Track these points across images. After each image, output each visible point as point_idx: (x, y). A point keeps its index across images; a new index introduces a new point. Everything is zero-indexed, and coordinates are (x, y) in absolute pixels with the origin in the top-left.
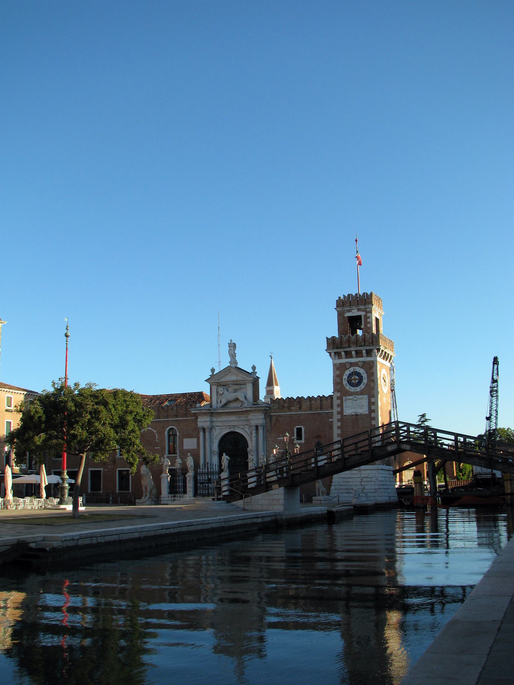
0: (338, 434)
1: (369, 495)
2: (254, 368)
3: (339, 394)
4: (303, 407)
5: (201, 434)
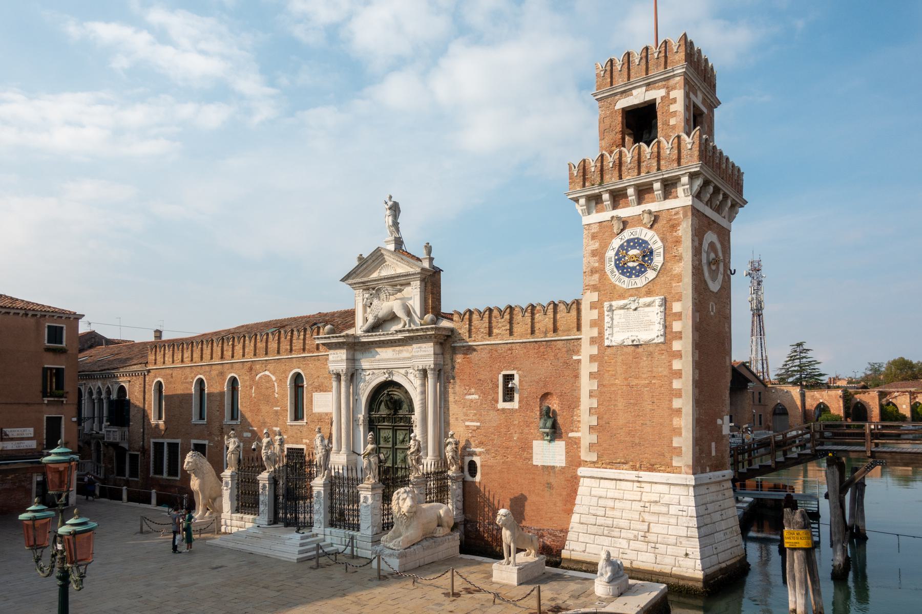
0: (591, 392)
1: (662, 548)
2: (429, 249)
3: (594, 296)
4: (517, 329)
5: (334, 384)
